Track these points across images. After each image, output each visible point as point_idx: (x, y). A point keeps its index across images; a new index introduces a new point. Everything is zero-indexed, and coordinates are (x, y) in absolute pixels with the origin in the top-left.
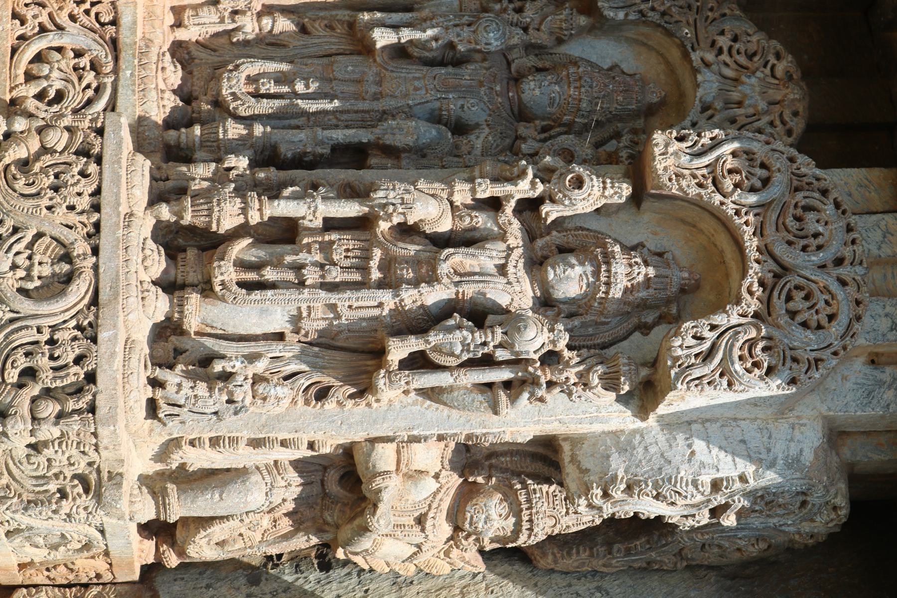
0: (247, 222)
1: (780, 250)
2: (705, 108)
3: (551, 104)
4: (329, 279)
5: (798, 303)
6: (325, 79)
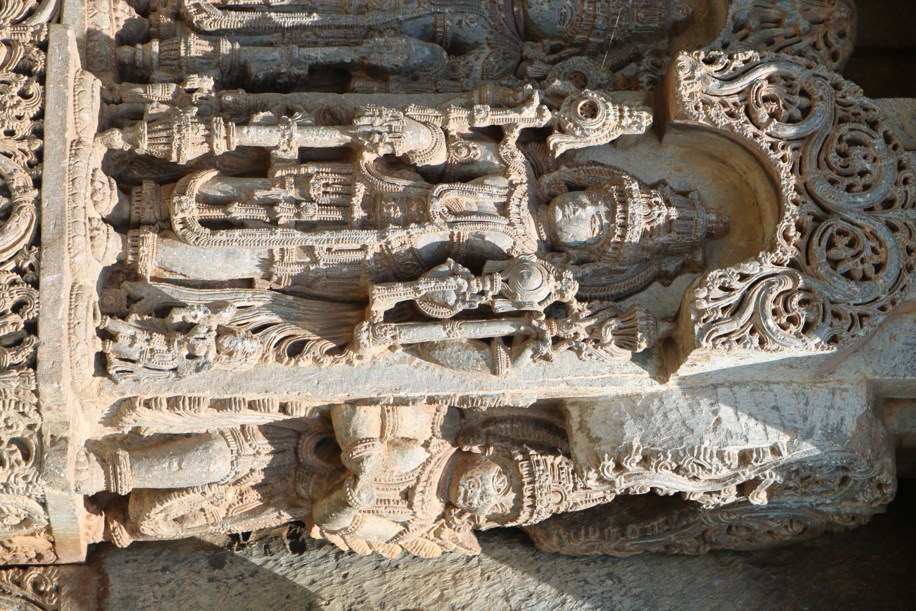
0: (212, 151)
1: (821, 189)
2: (739, 27)
3: (562, 21)
4: (305, 218)
5: (841, 250)
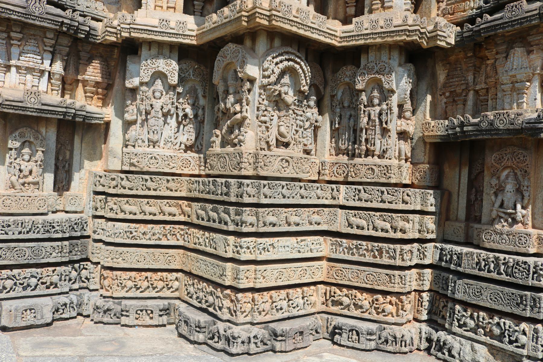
1: (374, 72)
5: (382, 70)
6: (343, 134)
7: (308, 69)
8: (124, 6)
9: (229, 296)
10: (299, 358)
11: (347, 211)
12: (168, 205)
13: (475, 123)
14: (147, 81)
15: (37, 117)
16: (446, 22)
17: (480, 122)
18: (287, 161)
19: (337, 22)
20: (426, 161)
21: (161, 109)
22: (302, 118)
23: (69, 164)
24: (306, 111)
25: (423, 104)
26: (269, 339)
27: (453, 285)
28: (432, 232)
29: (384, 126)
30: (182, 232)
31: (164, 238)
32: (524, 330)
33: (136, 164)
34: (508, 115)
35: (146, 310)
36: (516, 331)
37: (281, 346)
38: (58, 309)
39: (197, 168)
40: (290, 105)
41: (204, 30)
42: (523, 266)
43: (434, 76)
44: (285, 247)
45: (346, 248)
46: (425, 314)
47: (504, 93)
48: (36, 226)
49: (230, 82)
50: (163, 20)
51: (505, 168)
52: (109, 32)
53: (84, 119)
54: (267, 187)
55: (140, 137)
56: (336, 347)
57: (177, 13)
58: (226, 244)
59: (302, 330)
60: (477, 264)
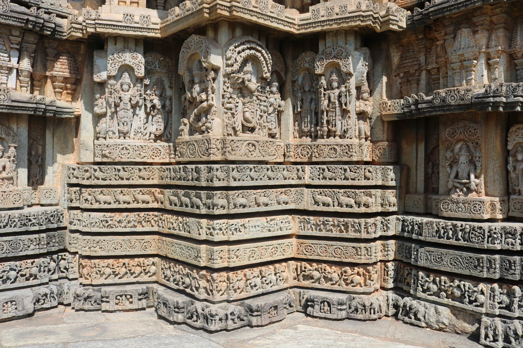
5: (339, 55)
6: (305, 117)
7: (269, 57)
8: (88, 3)
9: (205, 276)
10: (275, 331)
11: (313, 190)
12: (141, 193)
13: (429, 100)
14: (114, 74)
15: (7, 114)
16: (397, 7)
17: (433, 99)
18: (253, 145)
19: (294, 11)
20: (384, 139)
21: (130, 101)
22: (265, 104)
23: (42, 159)
24: (269, 97)
25: (380, 85)
26: (246, 314)
27: (415, 253)
28: (394, 205)
29: (344, 107)
30: (156, 219)
31: (139, 225)
32: (482, 290)
33: (108, 155)
34: (459, 92)
35: (126, 296)
36: (475, 291)
37: (257, 321)
38: (39, 299)
39: (168, 157)
40: (254, 92)
41: (168, 23)
42: (479, 231)
43: (388, 58)
44: (256, 227)
45: (314, 225)
46: (391, 283)
47: (454, 71)
48: (13, 220)
49: (195, 72)
50: (127, 15)
51: (458, 141)
52: (74, 28)
53: (55, 114)
54: (236, 170)
55: (111, 129)
56: (309, 318)
57: (140, 7)
58: (199, 227)
59: (276, 305)
60: (437, 232)
